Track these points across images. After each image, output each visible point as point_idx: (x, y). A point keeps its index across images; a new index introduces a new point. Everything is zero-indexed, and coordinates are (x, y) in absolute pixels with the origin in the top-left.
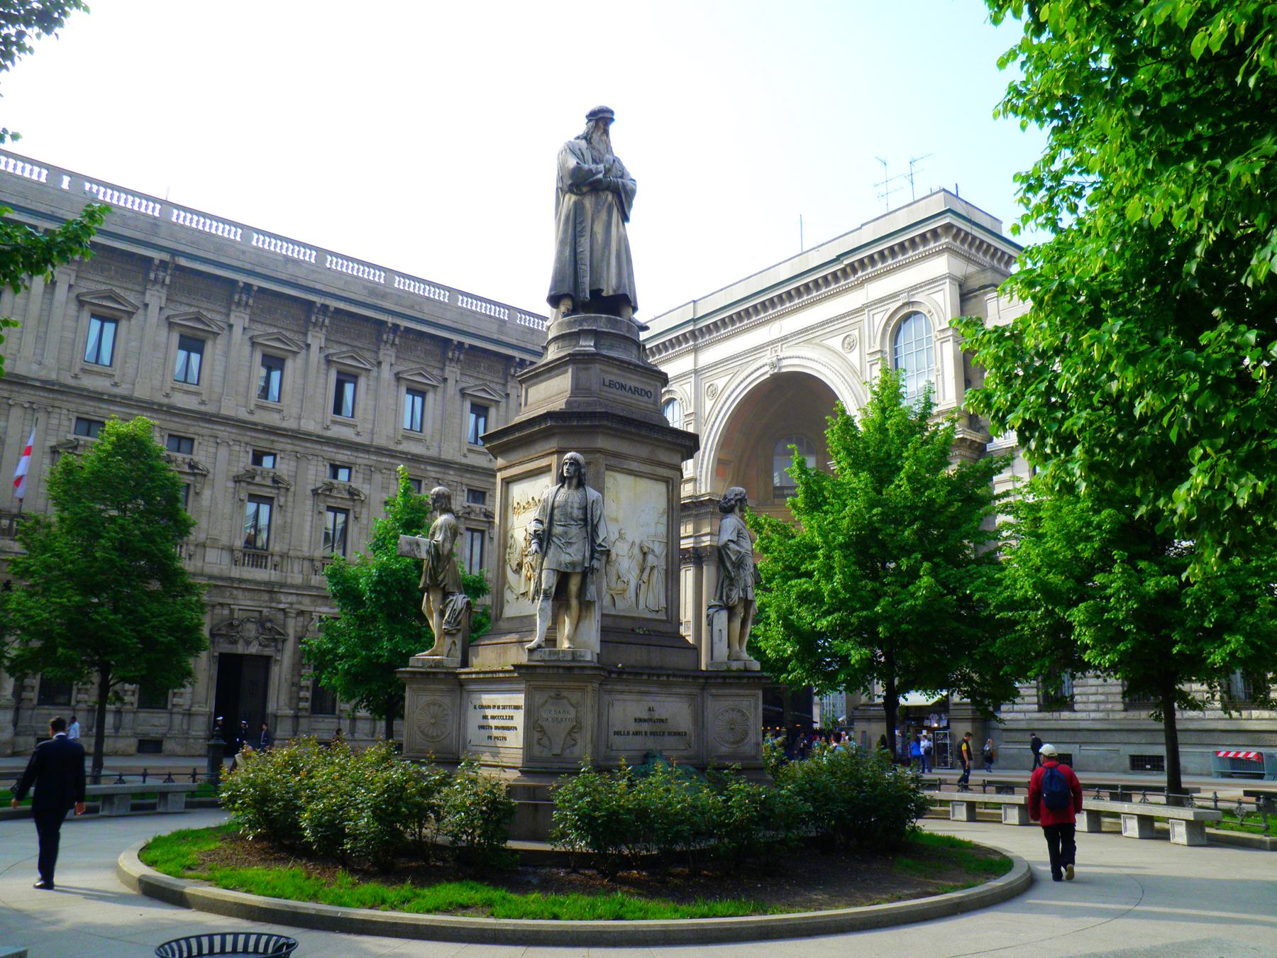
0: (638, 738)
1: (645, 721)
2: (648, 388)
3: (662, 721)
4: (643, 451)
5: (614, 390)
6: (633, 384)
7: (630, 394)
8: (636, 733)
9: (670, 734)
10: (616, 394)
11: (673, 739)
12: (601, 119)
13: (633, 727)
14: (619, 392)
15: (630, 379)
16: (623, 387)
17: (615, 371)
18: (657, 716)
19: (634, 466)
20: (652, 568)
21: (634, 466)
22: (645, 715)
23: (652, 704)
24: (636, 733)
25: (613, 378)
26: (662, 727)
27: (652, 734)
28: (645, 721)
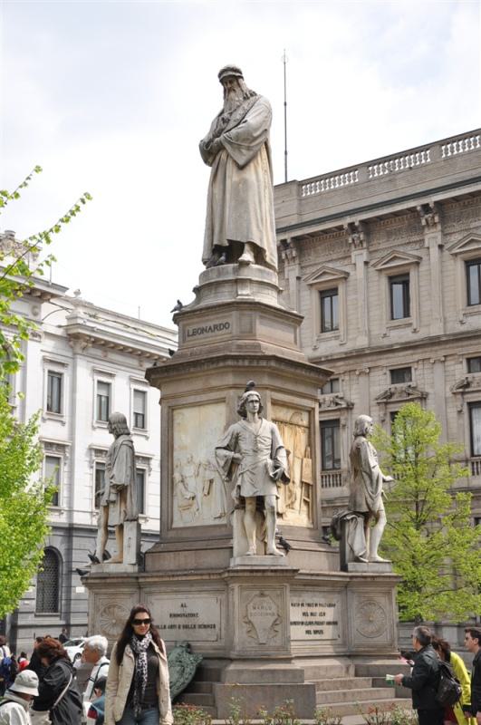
0: (173, 631)
1: (178, 615)
2: (224, 321)
3: (193, 615)
4: (199, 385)
5: (197, 336)
6: (211, 324)
7: (210, 334)
8: (172, 627)
9: (200, 627)
10: (201, 339)
11: (202, 631)
12: (230, 78)
13: (169, 621)
14: (202, 335)
15: (208, 320)
16: (203, 330)
17: (196, 320)
18: (188, 611)
19: (191, 399)
20: (211, 481)
21: (191, 399)
22: (179, 611)
23: (184, 601)
24: (172, 627)
25: (196, 327)
26: (190, 621)
27: (186, 627)
28: (178, 615)
